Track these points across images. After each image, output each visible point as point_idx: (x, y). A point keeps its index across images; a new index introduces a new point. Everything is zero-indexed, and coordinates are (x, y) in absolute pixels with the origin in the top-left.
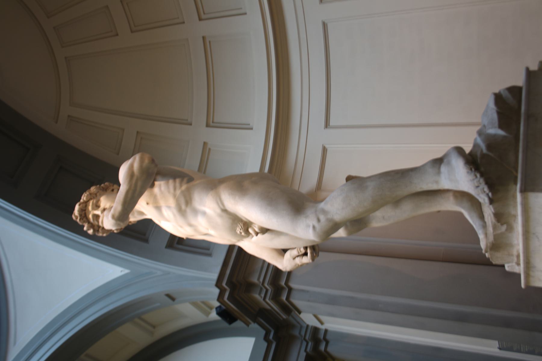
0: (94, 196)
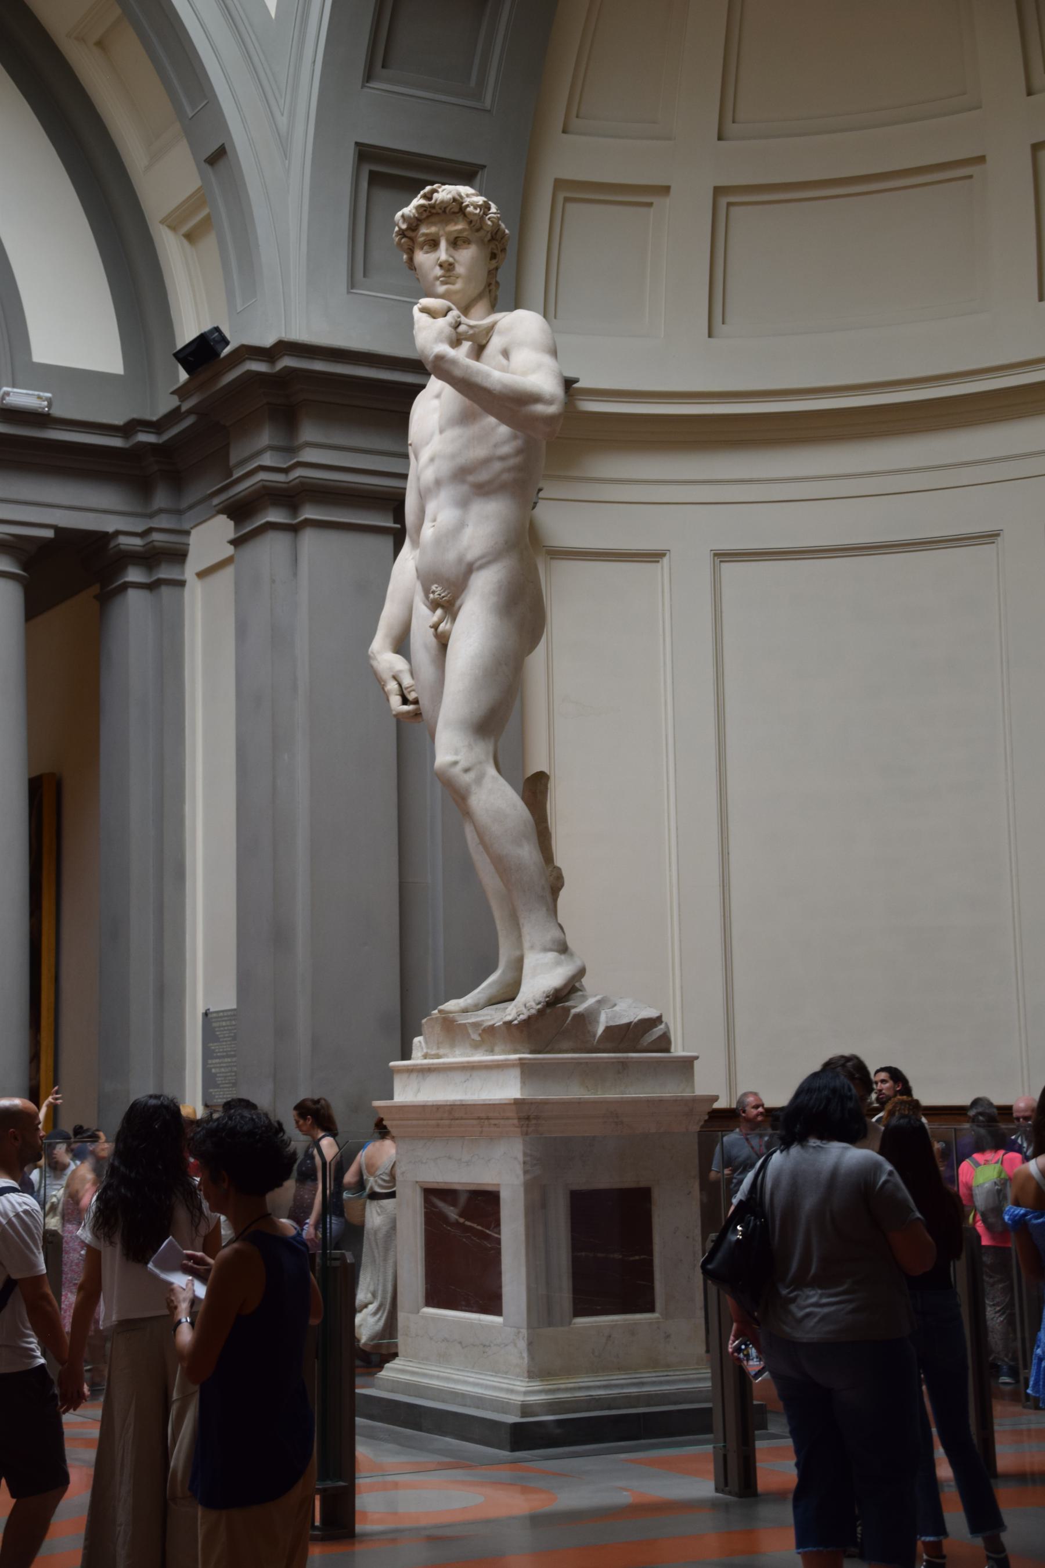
0: (478, 225)
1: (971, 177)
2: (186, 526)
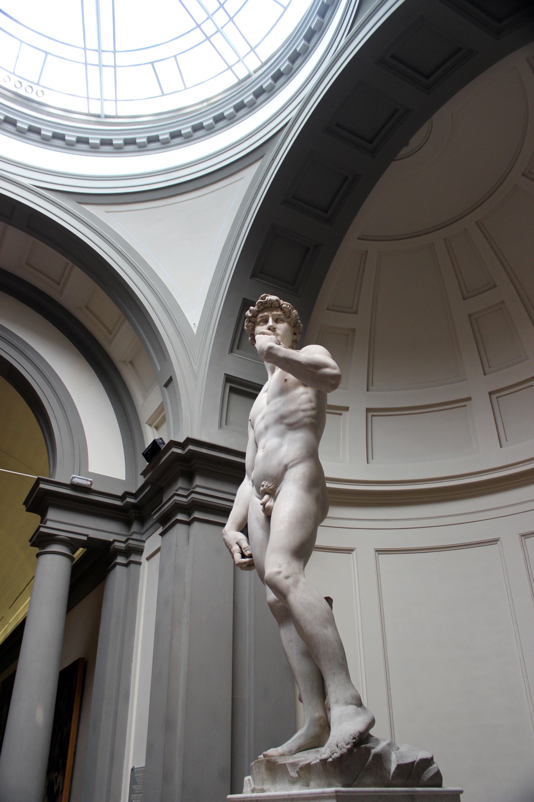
0: (288, 315)
1: (465, 406)
2: (144, 539)
